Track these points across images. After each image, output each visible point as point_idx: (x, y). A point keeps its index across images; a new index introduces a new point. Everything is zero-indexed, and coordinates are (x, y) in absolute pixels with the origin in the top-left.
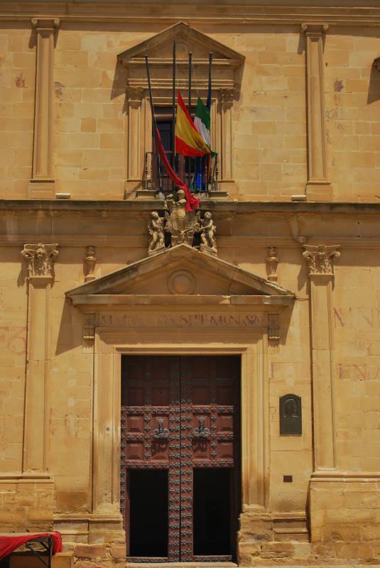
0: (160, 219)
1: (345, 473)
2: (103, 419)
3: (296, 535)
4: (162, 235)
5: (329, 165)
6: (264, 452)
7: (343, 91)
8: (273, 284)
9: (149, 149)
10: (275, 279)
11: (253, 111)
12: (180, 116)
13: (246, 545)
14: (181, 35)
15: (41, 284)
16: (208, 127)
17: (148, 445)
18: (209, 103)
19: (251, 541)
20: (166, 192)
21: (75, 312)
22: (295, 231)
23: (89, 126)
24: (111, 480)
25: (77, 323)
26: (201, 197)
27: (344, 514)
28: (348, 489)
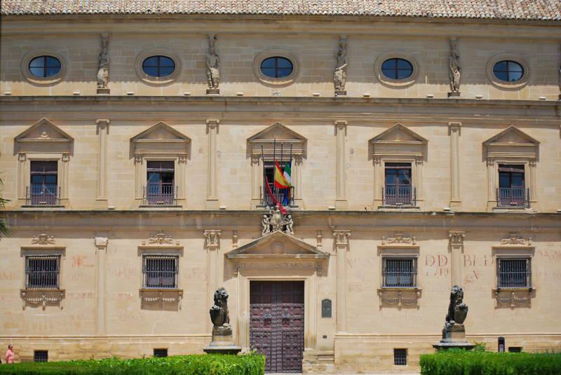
0: (268, 219)
1: (350, 334)
2: (242, 310)
4: (268, 226)
5: (347, 190)
7: (355, 153)
8: (319, 248)
9: (262, 185)
10: (321, 246)
11: (311, 164)
12: (277, 173)
13: (306, 366)
14: (277, 127)
15: (212, 249)
16: (290, 175)
17: (262, 322)
18: (291, 160)
19: (308, 364)
20: (270, 206)
21: (228, 261)
22: (330, 223)
23: (234, 172)
25: (230, 266)
26: (286, 208)
27: (350, 352)
28: (352, 341)
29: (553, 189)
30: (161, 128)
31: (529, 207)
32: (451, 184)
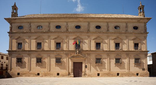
27: (90, 74)
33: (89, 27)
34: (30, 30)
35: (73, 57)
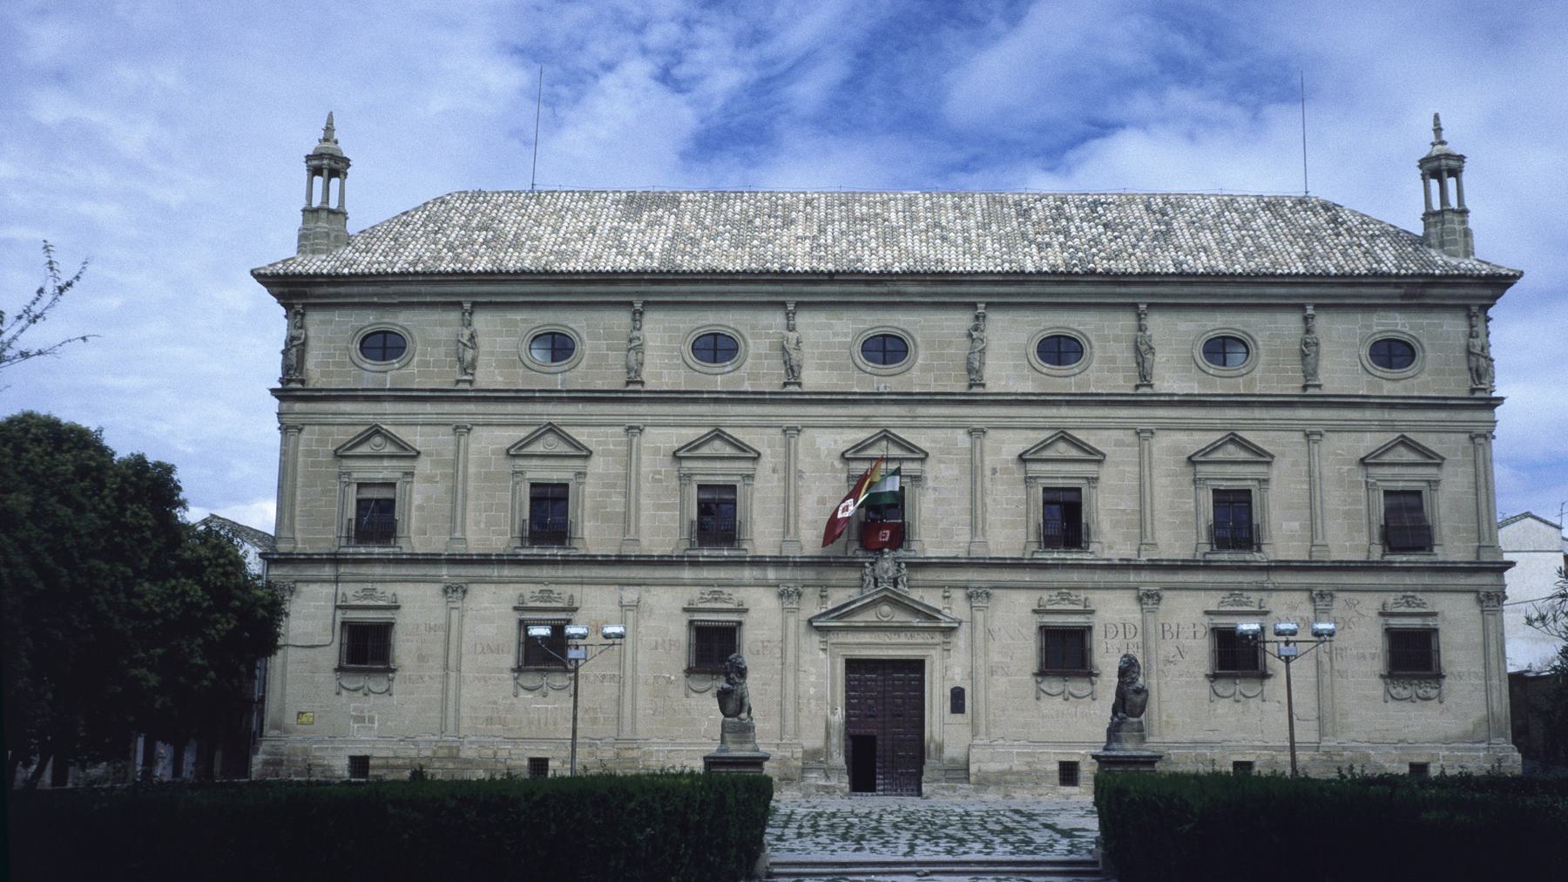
3: (960, 780)
6: (939, 722)
8: (946, 612)
11: (935, 489)
13: (925, 788)
15: (791, 611)
24: (837, 742)
27: (994, 767)
29: (1296, 525)
30: (718, 434)
31: (1259, 550)
32: (1142, 522)
33: (982, 351)
34: (469, 367)
35: (841, 612)
